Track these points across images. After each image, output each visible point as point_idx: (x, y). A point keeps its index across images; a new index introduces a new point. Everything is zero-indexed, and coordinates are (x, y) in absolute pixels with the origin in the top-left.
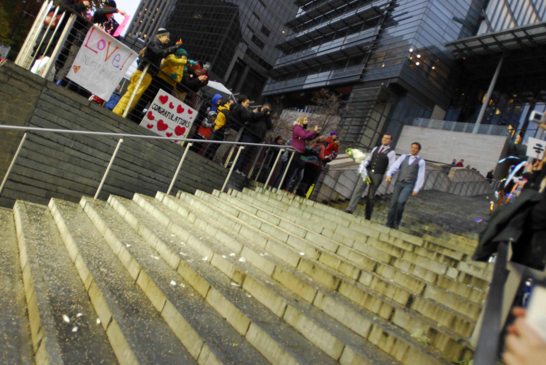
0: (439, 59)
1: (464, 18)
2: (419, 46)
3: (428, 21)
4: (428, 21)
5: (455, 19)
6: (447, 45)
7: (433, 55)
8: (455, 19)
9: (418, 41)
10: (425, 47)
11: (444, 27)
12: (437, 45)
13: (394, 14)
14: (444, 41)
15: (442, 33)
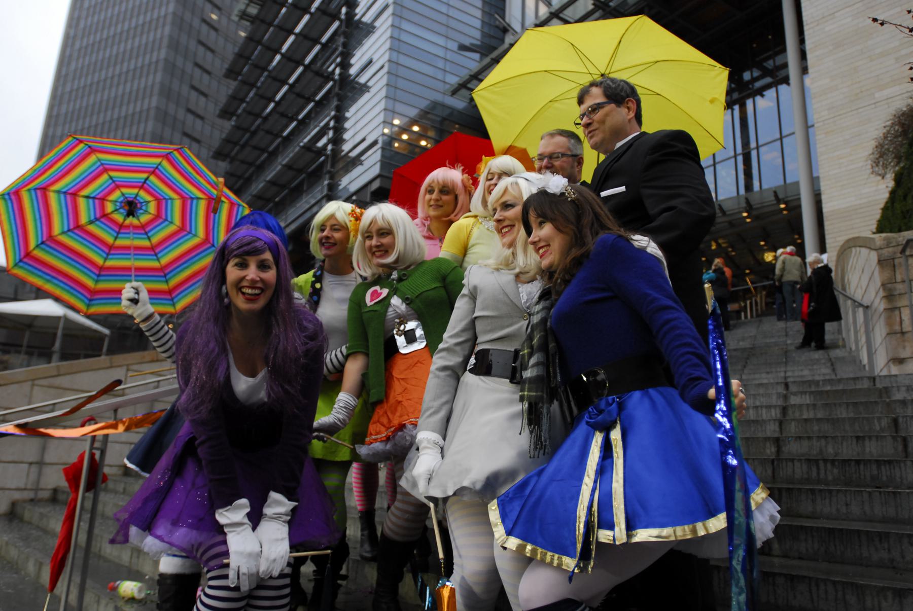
0: (458, 124)
1: (479, 43)
2: (413, 113)
3: (403, 60)
4: (403, 60)
5: (463, 48)
6: (454, 93)
7: (444, 119)
8: (463, 48)
9: (395, 100)
10: (422, 110)
11: (441, 64)
12: (439, 98)
13: (353, 71)
14: (447, 86)
15: (440, 76)
